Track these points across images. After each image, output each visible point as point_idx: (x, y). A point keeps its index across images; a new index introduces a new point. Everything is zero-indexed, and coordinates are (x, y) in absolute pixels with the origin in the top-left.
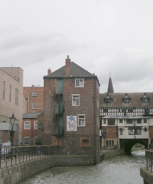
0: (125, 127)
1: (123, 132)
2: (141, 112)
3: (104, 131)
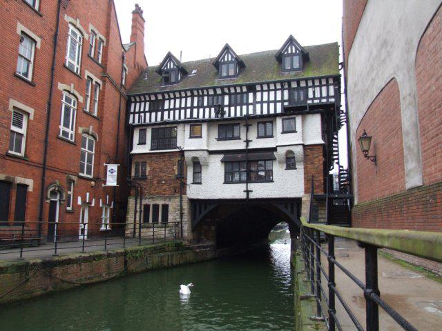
0: (211, 153)
1: (204, 172)
2: (275, 102)
3: (137, 170)
